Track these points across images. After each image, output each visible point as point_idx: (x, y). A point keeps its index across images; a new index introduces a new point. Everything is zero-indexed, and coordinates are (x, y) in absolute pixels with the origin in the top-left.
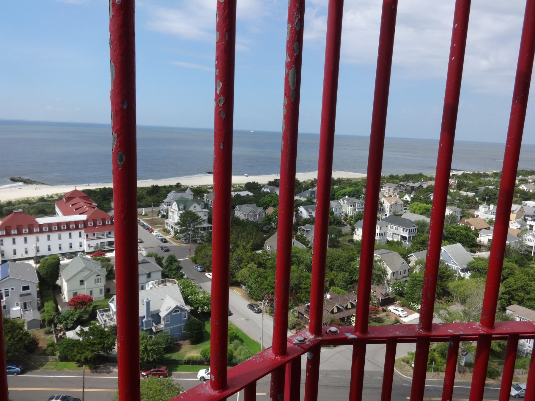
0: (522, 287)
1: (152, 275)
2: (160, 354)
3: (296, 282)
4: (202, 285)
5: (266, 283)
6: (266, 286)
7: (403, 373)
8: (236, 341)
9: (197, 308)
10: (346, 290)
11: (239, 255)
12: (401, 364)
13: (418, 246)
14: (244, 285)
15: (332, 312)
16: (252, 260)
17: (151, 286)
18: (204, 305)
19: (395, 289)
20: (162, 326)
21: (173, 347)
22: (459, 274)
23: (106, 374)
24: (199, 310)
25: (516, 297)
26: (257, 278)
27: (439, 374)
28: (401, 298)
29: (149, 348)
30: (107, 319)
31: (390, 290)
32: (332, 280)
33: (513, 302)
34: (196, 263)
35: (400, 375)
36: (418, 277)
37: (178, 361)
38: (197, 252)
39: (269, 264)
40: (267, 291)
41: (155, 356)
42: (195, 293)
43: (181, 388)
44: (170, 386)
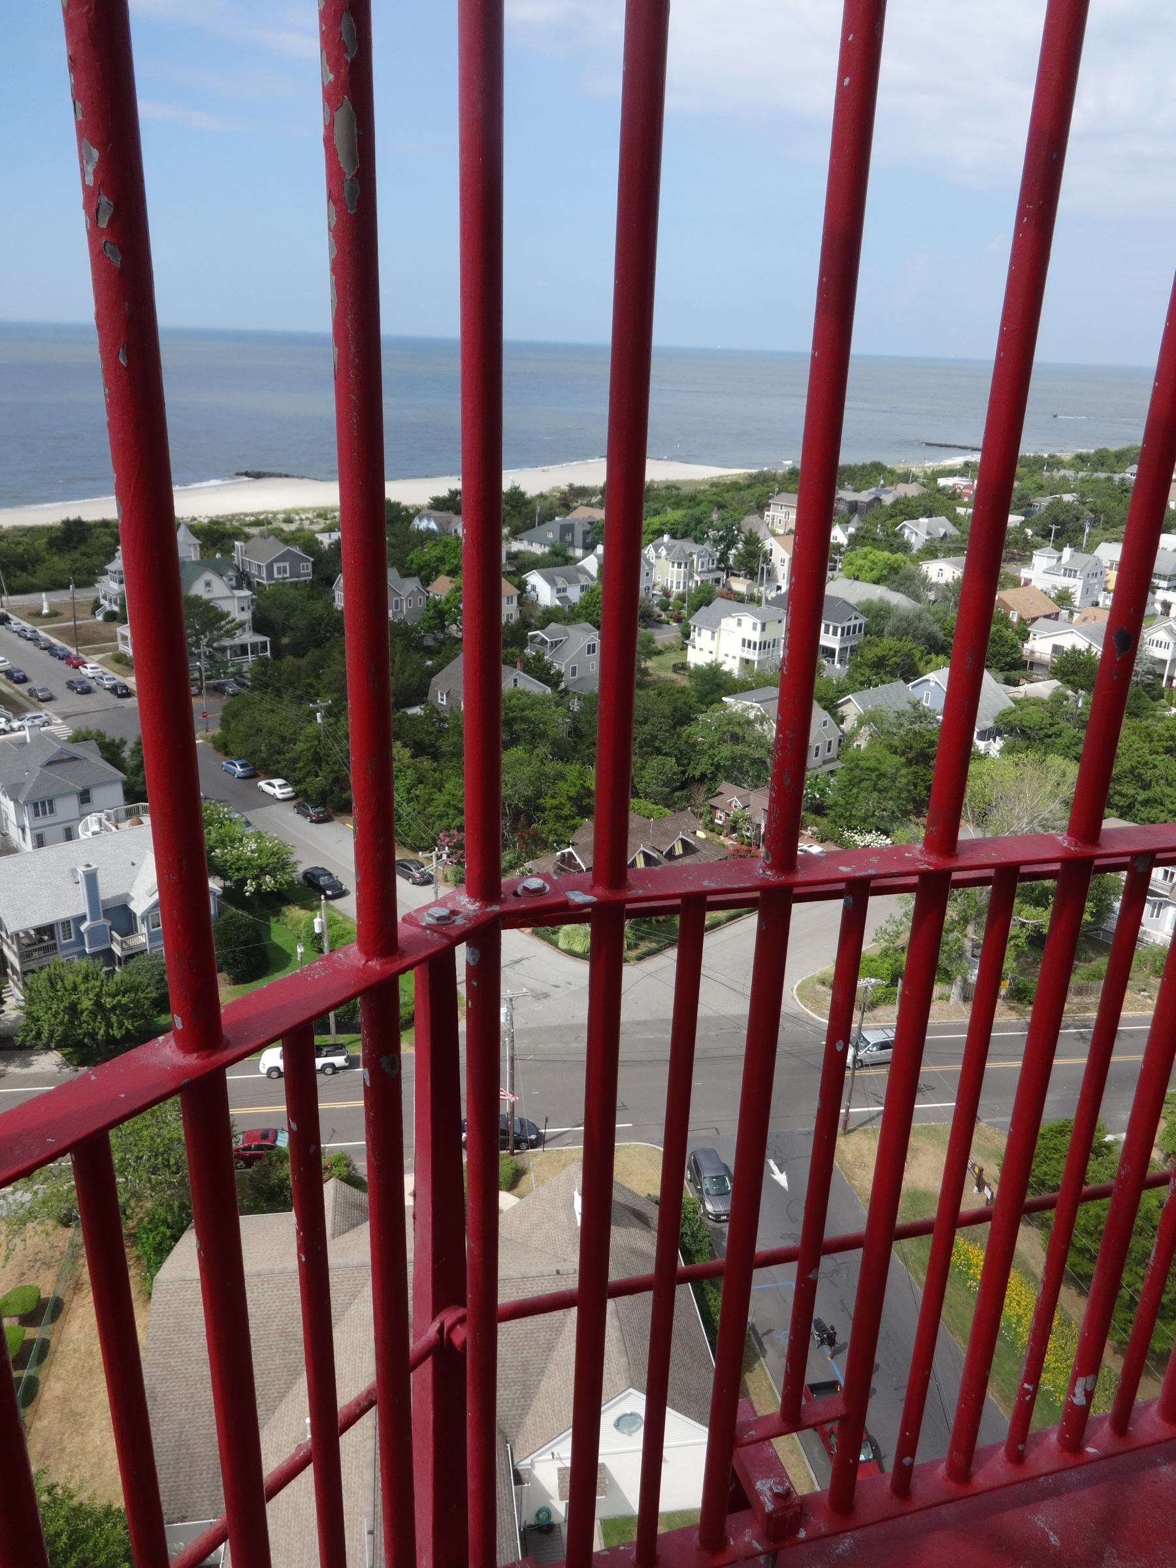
0: (1132, 770)
1: (95, 795)
2: (143, 1016)
3: (529, 792)
6: (441, 808)
9: (242, 882)
10: (667, 806)
12: (816, 992)
13: (867, 672)
17: (96, 828)
18: (263, 871)
24: (250, 888)
25: (1117, 798)
26: (414, 786)
28: (818, 819)
29: (108, 1002)
34: (227, 754)
35: (813, 1019)
36: (863, 759)
39: (445, 745)
40: (445, 822)
42: (232, 841)
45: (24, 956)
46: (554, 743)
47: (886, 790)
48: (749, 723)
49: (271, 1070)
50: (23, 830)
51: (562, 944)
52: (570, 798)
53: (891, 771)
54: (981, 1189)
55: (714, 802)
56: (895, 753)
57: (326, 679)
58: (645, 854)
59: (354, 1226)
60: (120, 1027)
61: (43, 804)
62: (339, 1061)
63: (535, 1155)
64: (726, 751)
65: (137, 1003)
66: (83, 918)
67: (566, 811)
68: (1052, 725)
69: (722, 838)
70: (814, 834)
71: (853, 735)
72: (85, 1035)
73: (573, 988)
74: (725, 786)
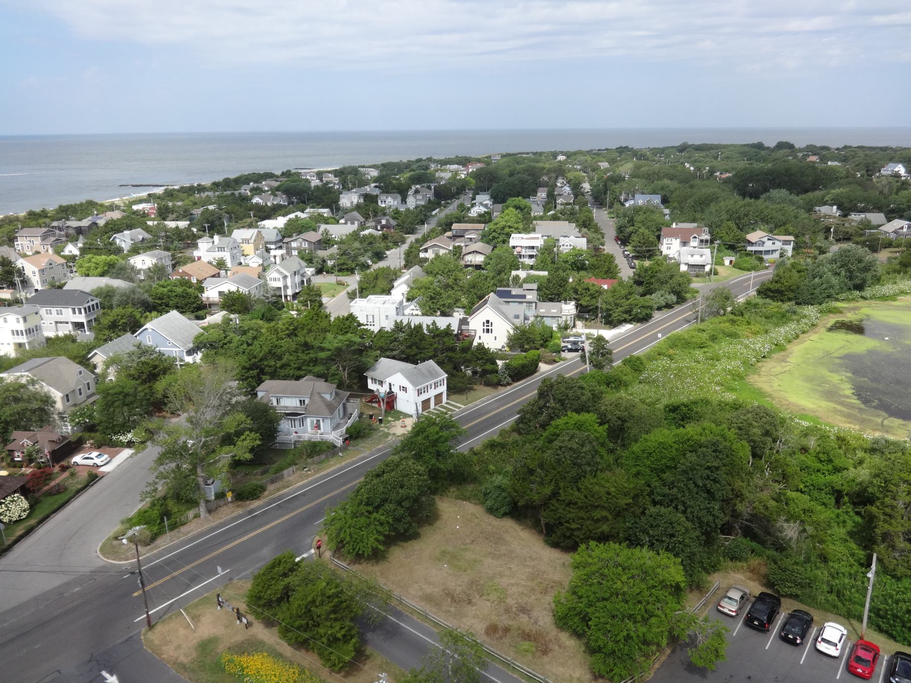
0: (270, 351)
7: (120, 560)
12: (113, 547)
13: (107, 332)
19: (78, 423)
22: (182, 360)
25: (267, 369)
28: (92, 434)
31: (68, 429)
33: (264, 377)
35: (115, 564)
36: (111, 388)
47: (132, 403)
48: (23, 386)
53: (131, 391)
54: (241, 621)
55: (10, 447)
56: (134, 378)
68: (225, 337)
69: (24, 469)
70: (92, 444)
71: (104, 375)
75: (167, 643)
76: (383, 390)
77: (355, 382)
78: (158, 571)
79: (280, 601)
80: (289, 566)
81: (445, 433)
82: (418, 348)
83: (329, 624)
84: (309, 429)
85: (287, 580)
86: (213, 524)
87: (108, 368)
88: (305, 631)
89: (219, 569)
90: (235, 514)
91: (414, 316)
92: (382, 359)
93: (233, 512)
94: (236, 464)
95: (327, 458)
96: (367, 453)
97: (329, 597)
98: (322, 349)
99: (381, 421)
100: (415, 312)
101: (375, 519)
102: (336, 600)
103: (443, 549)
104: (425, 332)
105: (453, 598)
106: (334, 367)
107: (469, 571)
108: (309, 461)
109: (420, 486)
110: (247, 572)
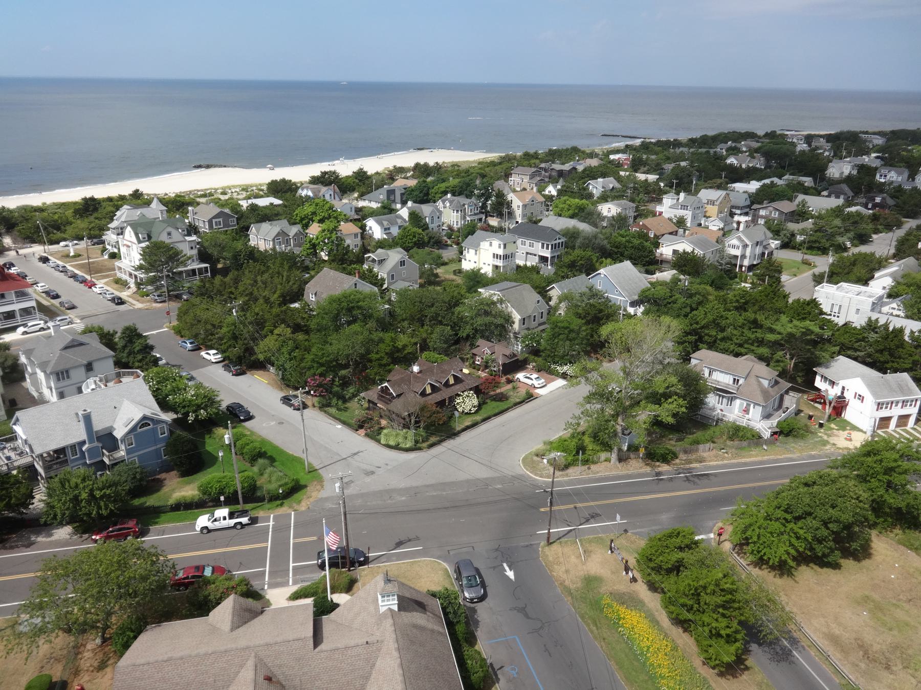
0: (714, 320)
1: (96, 366)
2: (122, 501)
3: (362, 351)
4: (194, 373)
5: (309, 357)
8: (261, 461)
9: (186, 415)
10: (447, 355)
11: (258, 314)
12: (533, 461)
13: (565, 270)
14: (273, 366)
15: (423, 394)
16: (283, 321)
17: (93, 386)
18: (199, 407)
20: (123, 453)
21: (147, 483)
22: (625, 310)
23: (24, 549)
24: (191, 418)
25: (706, 337)
26: (293, 351)
27: (589, 468)
29: (98, 494)
30: (12, 454)
32: (425, 340)
33: (701, 345)
34: (182, 337)
37: (159, 507)
38: (182, 314)
39: (313, 324)
40: (312, 371)
41: (111, 506)
43: (159, 552)
44: (139, 552)
45: (47, 468)
46: (378, 320)
47: (574, 339)
48: (494, 303)
49: (203, 528)
50: (51, 389)
51: (383, 442)
52: (387, 354)
53: (576, 328)
54: (627, 573)
55: (474, 351)
57: (241, 288)
58: (431, 385)
59: (246, 623)
60: (106, 507)
61: (62, 373)
62: (245, 520)
63: (364, 570)
64: (480, 321)
65: (117, 494)
66: (84, 443)
67: (384, 362)
68: (671, 297)
71: (556, 308)
72: (84, 514)
73: (389, 467)
74: (481, 342)
75: (559, 563)
76: (833, 392)
77: (802, 377)
78: (567, 496)
79: (669, 571)
80: (687, 541)
81: (905, 464)
82: (891, 355)
83: (715, 616)
84: (736, 411)
85: (681, 555)
86: (620, 473)
87: (560, 302)
88: (688, 611)
89: (618, 517)
90: (642, 471)
91: (894, 316)
92: (841, 357)
93: (641, 468)
94: (657, 422)
95: (749, 446)
96: (794, 454)
97: (723, 590)
98: (772, 331)
99: (821, 425)
100: (895, 312)
101: (792, 529)
102: (730, 596)
103: (867, 593)
104: (906, 338)
105: (866, 653)
106: (781, 353)
107: (895, 632)
108: (729, 443)
109: (857, 513)
110: (643, 530)
